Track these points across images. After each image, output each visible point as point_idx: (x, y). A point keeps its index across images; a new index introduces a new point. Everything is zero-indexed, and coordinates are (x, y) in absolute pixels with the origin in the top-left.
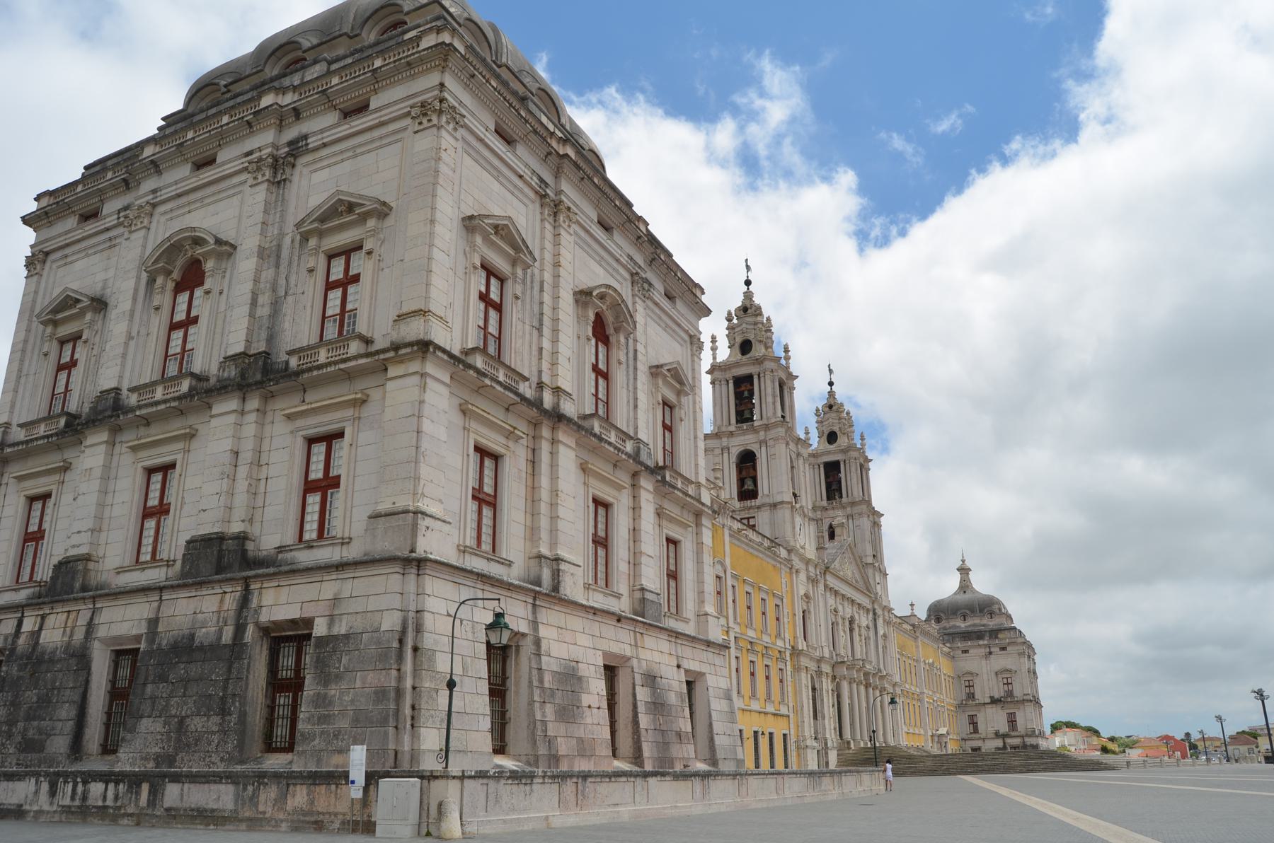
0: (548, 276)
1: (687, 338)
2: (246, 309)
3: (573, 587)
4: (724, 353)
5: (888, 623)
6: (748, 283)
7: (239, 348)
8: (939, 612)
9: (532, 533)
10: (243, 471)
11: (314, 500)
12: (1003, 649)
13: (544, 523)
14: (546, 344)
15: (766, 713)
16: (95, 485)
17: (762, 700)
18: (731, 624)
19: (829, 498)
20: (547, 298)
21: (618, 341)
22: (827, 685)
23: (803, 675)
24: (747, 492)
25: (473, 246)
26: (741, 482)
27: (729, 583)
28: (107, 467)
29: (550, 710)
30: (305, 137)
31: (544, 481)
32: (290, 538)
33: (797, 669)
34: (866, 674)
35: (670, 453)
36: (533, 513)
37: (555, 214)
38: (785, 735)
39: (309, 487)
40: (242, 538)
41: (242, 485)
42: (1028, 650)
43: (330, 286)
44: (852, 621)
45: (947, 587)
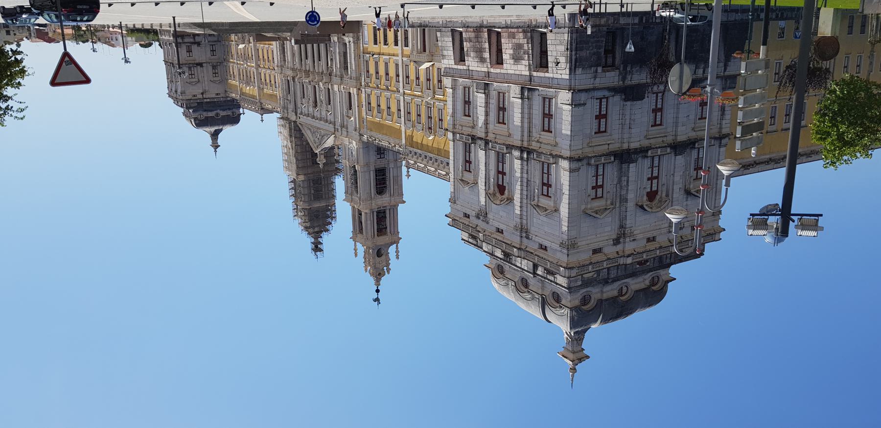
0: (525, 201)
2: (630, 179)
3: (515, 90)
6: (378, 291)
7: (631, 165)
8: (235, 120)
10: (628, 122)
11: (603, 112)
13: (526, 111)
14: (525, 175)
16: (680, 120)
17: (381, 60)
20: (525, 193)
23: (354, 75)
28: (677, 126)
29: (526, 47)
30: (614, 244)
32: (611, 99)
35: (467, 150)
36: (530, 114)
39: (605, 116)
40: (625, 100)
41: (628, 117)
42: (173, 94)
43: (602, 186)
44: (316, 106)
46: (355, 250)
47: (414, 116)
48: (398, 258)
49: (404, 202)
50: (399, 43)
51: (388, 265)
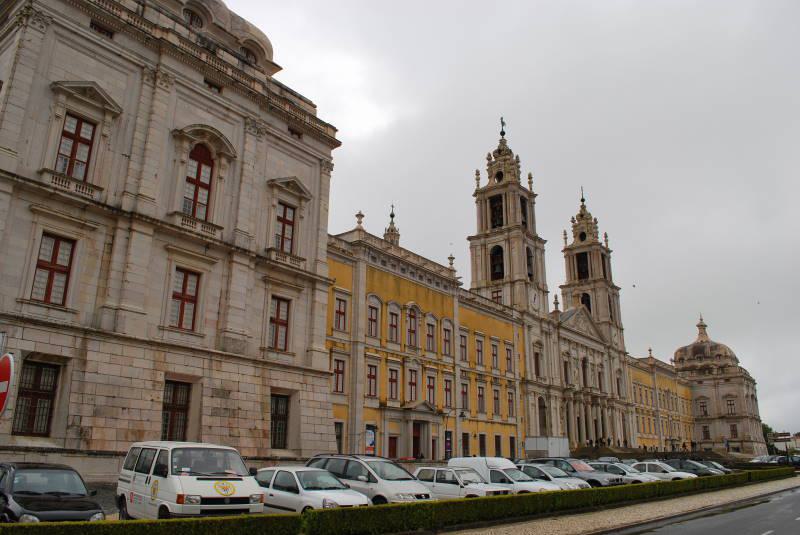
1: (317, 162)
4: (485, 182)
5: (623, 362)
6: (503, 133)
9: (103, 292)
12: (727, 380)
15: (493, 423)
17: (490, 414)
18: (457, 362)
19: (580, 278)
20: (139, 136)
21: (220, 164)
22: (555, 405)
24: (497, 273)
25: (57, 103)
26: (493, 267)
27: (457, 334)
31: (117, 257)
33: (525, 393)
34: (595, 398)
37: (155, 79)
38: (512, 439)
44: (585, 361)
45: (691, 338)
46: (530, 183)
47: (441, 336)
48: (478, 173)
49: (469, 239)
50: (460, 437)
51: (490, 165)
